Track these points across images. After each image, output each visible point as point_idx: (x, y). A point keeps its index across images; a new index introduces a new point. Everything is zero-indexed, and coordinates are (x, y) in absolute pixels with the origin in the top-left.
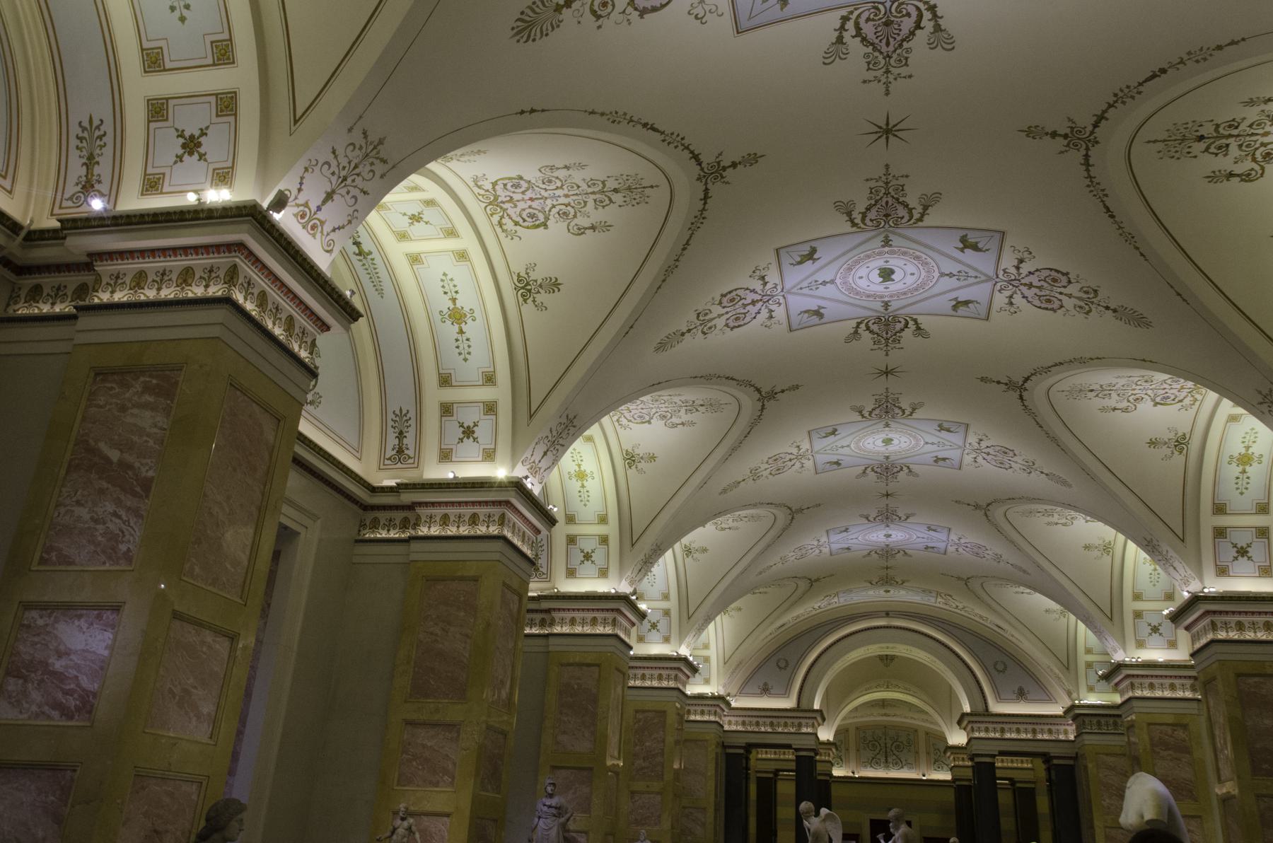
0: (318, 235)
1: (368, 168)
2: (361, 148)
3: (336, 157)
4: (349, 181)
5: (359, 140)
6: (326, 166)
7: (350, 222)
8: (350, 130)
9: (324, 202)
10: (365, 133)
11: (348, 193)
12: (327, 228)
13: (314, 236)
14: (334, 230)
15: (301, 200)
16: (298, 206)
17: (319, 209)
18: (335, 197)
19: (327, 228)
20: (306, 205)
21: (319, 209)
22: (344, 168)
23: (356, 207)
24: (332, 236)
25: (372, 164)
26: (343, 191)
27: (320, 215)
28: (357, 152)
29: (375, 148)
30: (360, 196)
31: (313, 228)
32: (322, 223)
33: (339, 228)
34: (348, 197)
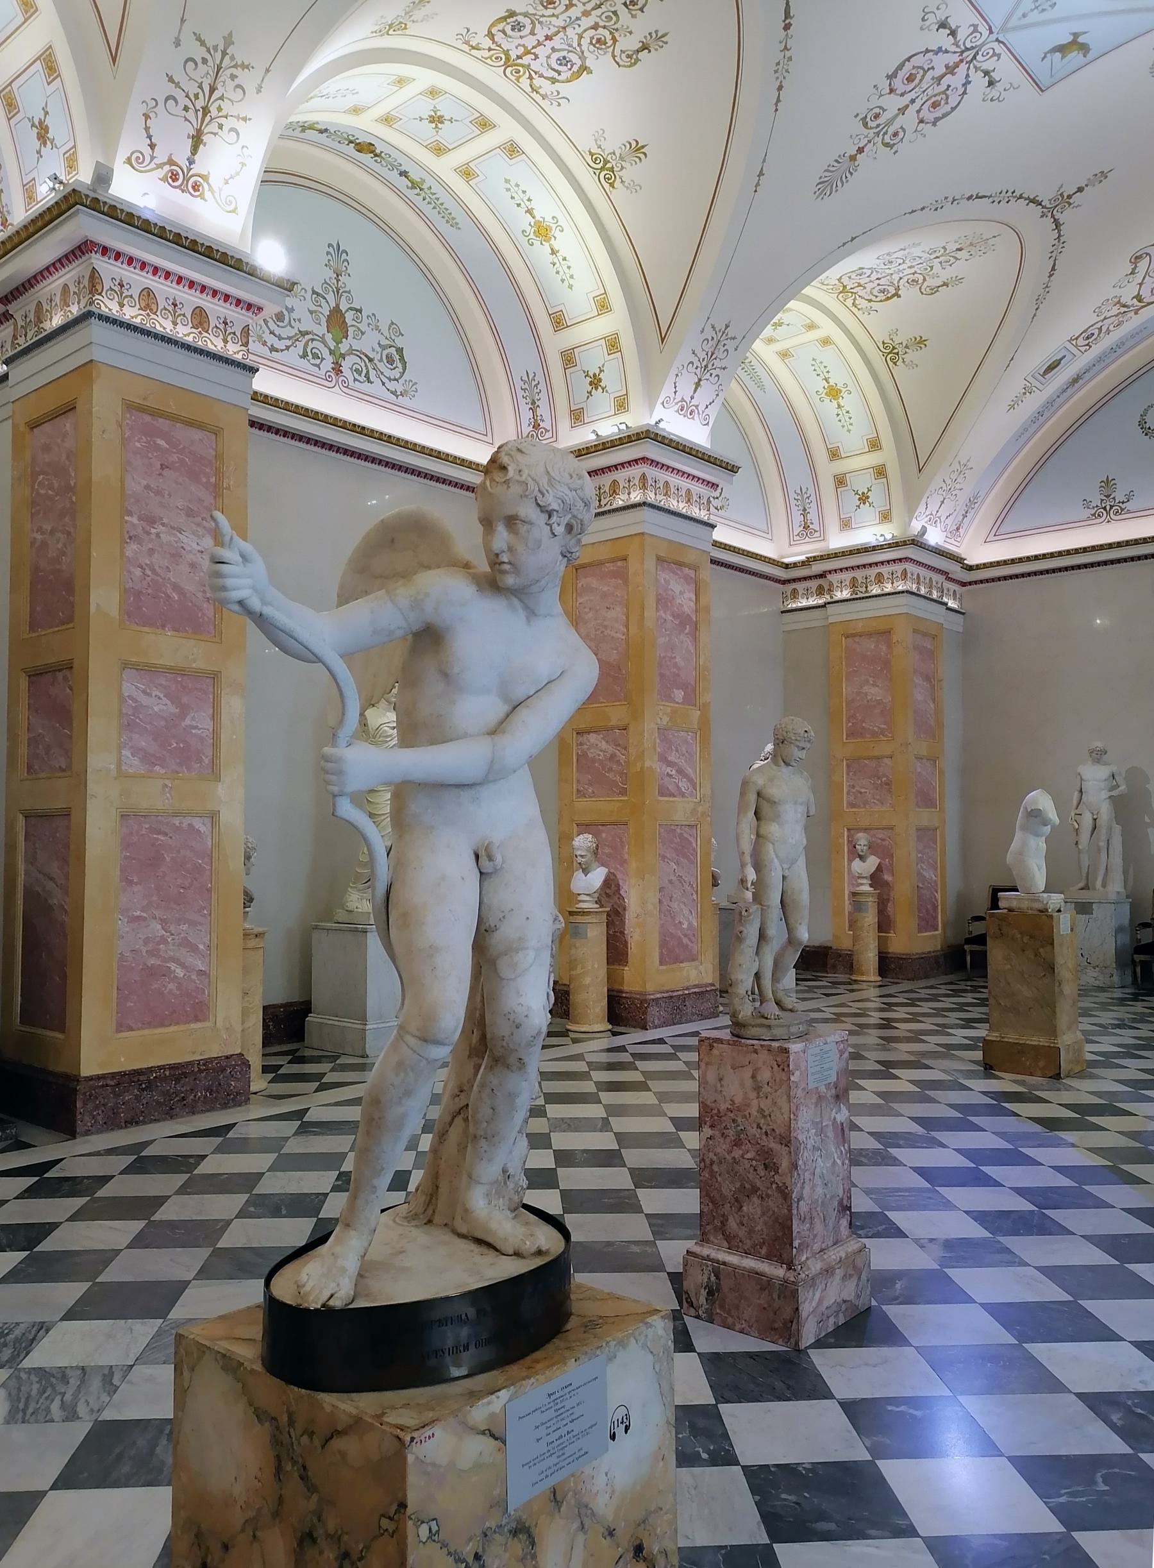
1: (230, 84)
2: (205, 61)
3: (177, 85)
5: (199, 53)
6: (171, 102)
8: (177, 43)
10: (199, 39)
13: (202, 197)
15: (161, 158)
16: (160, 166)
18: (205, 138)
20: (171, 162)
22: (197, 96)
23: (241, 142)
25: (233, 77)
28: (202, 68)
29: (224, 53)
31: (196, 187)
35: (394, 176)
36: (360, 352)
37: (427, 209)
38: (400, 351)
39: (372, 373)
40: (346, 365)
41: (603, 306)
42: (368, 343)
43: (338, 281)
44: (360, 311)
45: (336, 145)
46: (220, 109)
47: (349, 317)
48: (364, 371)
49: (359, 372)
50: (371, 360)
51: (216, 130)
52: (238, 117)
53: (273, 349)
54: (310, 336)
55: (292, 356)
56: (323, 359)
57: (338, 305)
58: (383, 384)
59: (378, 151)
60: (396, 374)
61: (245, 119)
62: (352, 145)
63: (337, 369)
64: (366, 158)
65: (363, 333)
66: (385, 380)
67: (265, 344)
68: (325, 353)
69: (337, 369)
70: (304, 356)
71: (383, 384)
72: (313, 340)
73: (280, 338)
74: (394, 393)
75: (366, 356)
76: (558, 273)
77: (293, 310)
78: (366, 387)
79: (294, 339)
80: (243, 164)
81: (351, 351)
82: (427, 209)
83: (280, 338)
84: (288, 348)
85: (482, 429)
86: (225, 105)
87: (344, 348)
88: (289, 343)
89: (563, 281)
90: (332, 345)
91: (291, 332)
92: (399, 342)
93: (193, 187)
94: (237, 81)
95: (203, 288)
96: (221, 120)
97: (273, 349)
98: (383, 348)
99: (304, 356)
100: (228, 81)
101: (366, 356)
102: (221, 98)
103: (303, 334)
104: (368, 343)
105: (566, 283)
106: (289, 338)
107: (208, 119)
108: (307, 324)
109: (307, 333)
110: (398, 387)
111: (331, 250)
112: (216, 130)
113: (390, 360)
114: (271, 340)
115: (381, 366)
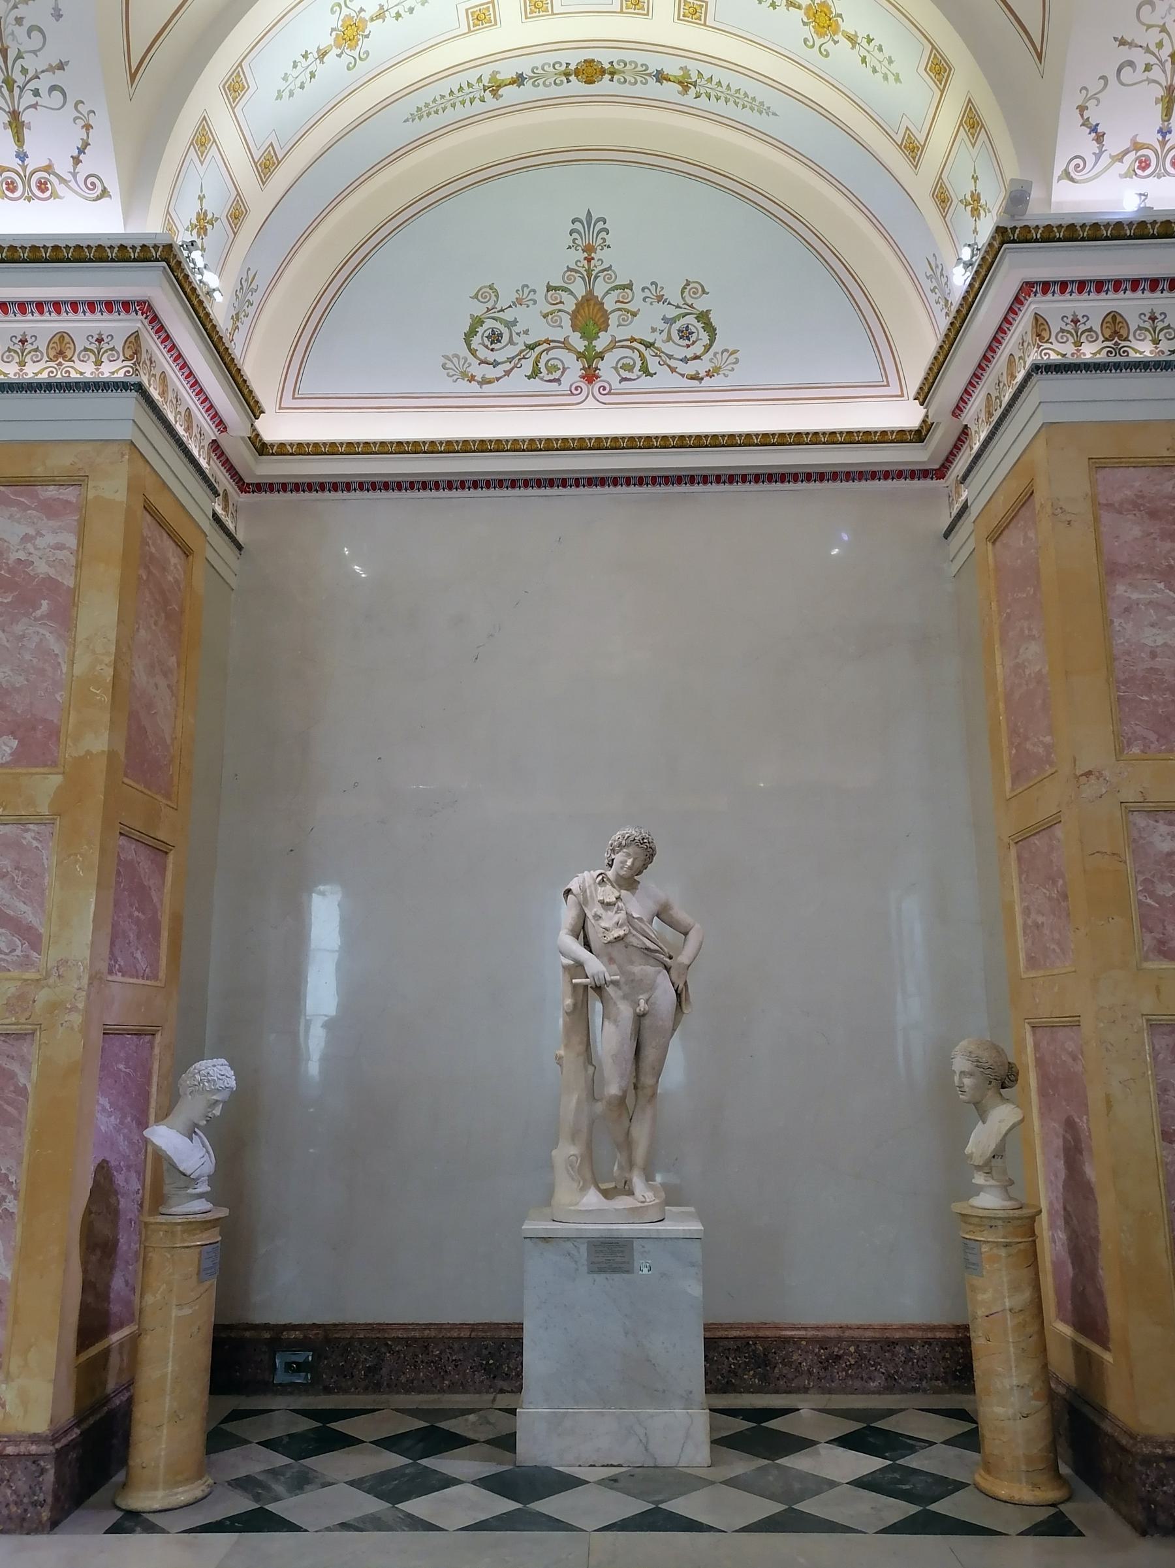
0: (61, 189)
1: (21, 32)
4: (19, 79)
7: (88, 127)
9: (19, 139)
11: (36, 93)
12: (63, 167)
13: (54, 195)
14: (77, 161)
17: (22, 156)
18: (24, 118)
19: (63, 167)
21: (22, 156)
24: (83, 170)
25: (19, 21)
26: (28, 98)
27: (32, 163)
30: (58, 78)
31: (42, 186)
32: (48, 169)
33: (81, 151)
34: (44, 99)
35: (653, 89)
36: (633, 340)
37: (730, 110)
38: (703, 317)
39: (653, 364)
40: (605, 368)
41: (940, 69)
42: (648, 321)
43: (589, 260)
44: (630, 286)
45: (554, 91)
46: (24, 71)
47: (609, 305)
48: (639, 363)
49: (630, 369)
50: (649, 345)
51: (33, 100)
52: (51, 69)
53: (485, 381)
54: (545, 346)
55: (518, 380)
56: (564, 369)
57: (590, 293)
58: (673, 370)
59: (607, 66)
60: (698, 349)
61: (61, 66)
62: (573, 78)
63: (590, 376)
64: (604, 85)
65: (634, 314)
66: (673, 363)
67: (472, 379)
68: (569, 359)
69: (590, 376)
70: (535, 373)
71: (673, 370)
72: (547, 350)
73: (495, 364)
74: (695, 377)
75: (642, 342)
76: (875, 71)
77: (515, 322)
78: (645, 382)
79: (515, 361)
80: (88, 127)
81: (614, 345)
82: (720, 107)
83: (495, 364)
84: (508, 373)
85: (877, 377)
86: (29, 62)
87: (600, 344)
88: (508, 366)
89: (886, 78)
90: (580, 344)
91: (512, 351)
92: (701, 305)
93: (39, 188)
94: (27, 24)
95: (57, 306)
96: (33, 85)
97: (485, 381)
98: (670, 321)
99: (535, 373)
100: (17, 29)
101: (642, 342)
102: (19, 56)
103: (531, 347)
104: (648, 321)
105: (891, 78)
106: (510, 360)
107: (16, 91)
108: (541, 331)
109: (539, 344)
110: (701, 367)
111: (578, 226)
112: (33, 100)
113: (685, 333)
114: (480, 371)
115: (668, 348)
